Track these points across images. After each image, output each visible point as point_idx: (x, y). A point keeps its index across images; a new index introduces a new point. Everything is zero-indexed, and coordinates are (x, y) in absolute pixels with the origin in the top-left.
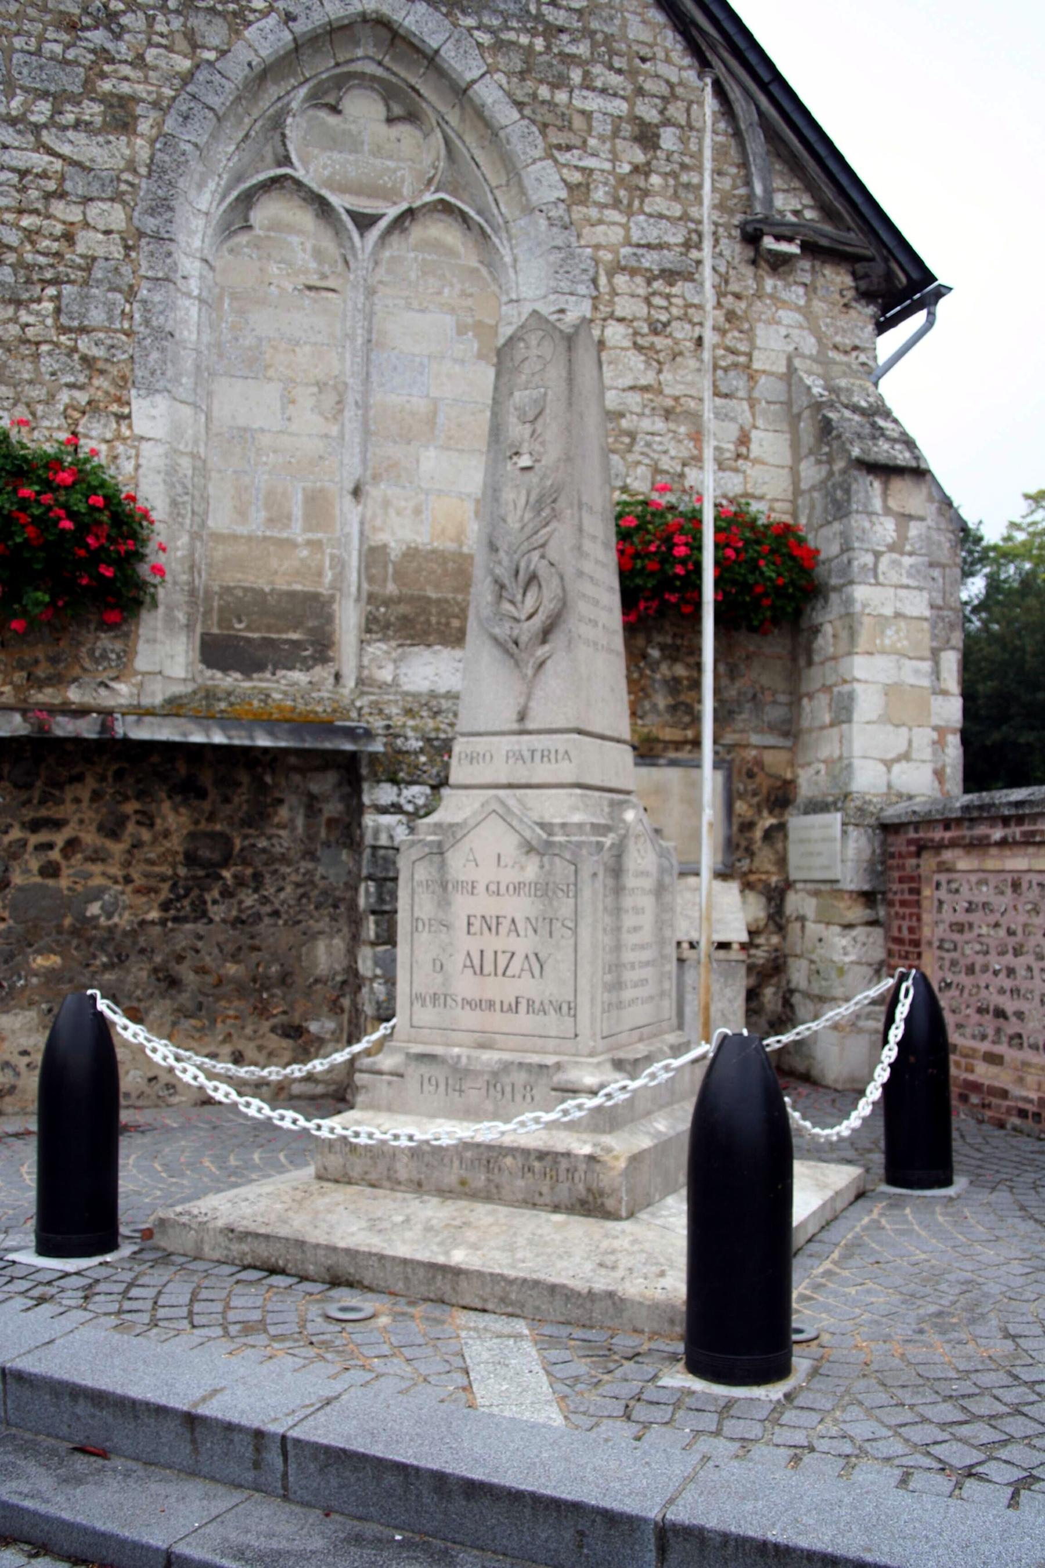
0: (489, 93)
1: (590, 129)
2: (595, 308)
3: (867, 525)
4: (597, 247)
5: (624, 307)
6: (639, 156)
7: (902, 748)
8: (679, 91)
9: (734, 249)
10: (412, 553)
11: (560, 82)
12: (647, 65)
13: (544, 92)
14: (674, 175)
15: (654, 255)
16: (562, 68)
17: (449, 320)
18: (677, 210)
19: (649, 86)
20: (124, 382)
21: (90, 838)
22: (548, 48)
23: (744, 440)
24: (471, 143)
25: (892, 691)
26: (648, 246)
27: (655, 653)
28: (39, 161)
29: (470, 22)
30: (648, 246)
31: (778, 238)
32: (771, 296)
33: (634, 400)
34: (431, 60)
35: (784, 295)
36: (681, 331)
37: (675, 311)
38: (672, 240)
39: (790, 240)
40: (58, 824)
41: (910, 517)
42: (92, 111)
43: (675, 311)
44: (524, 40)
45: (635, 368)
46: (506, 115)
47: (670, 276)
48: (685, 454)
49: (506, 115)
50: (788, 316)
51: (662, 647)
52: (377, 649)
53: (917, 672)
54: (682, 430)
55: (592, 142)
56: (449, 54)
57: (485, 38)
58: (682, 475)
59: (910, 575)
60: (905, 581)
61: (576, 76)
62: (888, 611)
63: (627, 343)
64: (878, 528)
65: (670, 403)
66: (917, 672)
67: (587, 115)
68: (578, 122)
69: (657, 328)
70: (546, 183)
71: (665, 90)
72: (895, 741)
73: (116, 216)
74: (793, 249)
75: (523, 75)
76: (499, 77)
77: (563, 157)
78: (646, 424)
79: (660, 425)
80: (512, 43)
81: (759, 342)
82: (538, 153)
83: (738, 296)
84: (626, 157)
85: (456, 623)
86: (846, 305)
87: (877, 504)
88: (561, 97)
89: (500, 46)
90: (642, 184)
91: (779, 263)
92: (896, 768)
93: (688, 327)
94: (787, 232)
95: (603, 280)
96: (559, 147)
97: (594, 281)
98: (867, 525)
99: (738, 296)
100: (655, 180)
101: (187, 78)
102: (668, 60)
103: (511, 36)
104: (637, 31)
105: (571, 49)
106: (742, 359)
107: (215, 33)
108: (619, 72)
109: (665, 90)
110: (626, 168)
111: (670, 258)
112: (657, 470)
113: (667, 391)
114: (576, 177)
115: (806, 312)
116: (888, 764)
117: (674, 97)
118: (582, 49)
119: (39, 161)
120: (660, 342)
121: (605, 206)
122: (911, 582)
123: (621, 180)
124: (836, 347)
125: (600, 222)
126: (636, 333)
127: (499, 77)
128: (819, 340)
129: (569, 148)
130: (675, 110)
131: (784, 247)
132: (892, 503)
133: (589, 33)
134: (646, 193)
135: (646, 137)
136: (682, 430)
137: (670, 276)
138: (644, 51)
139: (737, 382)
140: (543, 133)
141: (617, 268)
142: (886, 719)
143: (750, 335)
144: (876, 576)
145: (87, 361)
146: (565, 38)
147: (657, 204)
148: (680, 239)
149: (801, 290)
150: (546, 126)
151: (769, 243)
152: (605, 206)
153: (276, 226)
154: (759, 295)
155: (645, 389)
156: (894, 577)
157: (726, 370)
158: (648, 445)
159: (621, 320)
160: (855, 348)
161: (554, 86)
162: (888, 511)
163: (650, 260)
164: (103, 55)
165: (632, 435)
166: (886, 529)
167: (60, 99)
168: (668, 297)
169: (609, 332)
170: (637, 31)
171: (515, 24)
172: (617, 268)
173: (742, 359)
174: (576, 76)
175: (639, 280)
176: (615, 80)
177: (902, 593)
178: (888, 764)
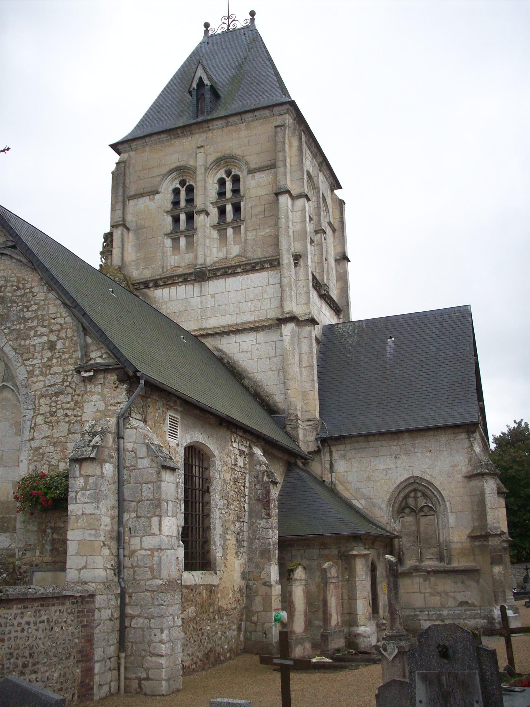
1: (35, 349)
2: (34, 412)
3: (74, 482)
4: (36, 391)
6: (49, 354)
7: (84, 564)
8: (64, 326)
9: (76, 378)
11: (28, 337)
12: (55, 321)
13: (23, 342)
14: (60, 357)
15: (53, 388)
16: (28, 332)
17: (8, 423)
18: (61, 369)
19: (54, 328)
22: (24, 327)
25: (80, 542)
26: (51, 386)
27: (49, 531)
29: (3, 327)
30: (51, 386)
31: (86, 371)
32: (90, 392)
33: (45, 440)
35: (94, 390)
36: (60, 413)
37: (58, 406)
38: (58, 381)
39: (90, 371)
41: (89, 476)
43: (58, 406)
44: (18, 327)
45: (45, 430)
47: (57, 394)
48: (59, 457)
50: (95, 398)
51: (51, 528)
53: (90, 534)
54: (59, 449)
55: (36, 354)
57: (6, 331)
58: (58, 465)
59: (88, 498)
60: (87, 500)
61: (32, 333)
62: (80, 513)
63: (43, 422)
64: (78, 482)
65: (56, 440)
66: (90, 534)
67: (34, 346)
68: (32, 349)
69: (52, 414)
71: (59, 327)
72: (80, 562)
74: (91, 374)
75: (17, 339)
76: (10, 342)
77: (26, 363)
78: (48, 450)
79: (52, 449)
80: (14, 329)
81: (85, 411)
82: (20, 364)
83: (79, 395)
84: (45, 356)
85: (6, 524)
86: (116, 387)
87: (77, 474)
88: (27, 342)
89: (12, 331)
90: (50, 364)
91: (89, 380)
92: (82, 572)
93: (62, 411)
94: (88, 368)
95: (37, 402)
96: (26, 360)
97: (34, 403)
98: (74, 482)
99: (79, 395)
100: (54, 361)
102: (61, 316)
103: (14, 327)
105: (32, 325)
106: (79, 418)
108: (45, 327)
109: (59, 327)
110: (46, 360)
113: (55, 436)
114: (30, 368)
115: (102, 394)
116: (79, 570)
117: (62, 328)
118: (35, 323)
120: (53, 419)
121: (38, 376)
122: (89, 501)
123: (44, 365)
124: (111, 405)
125: (37, 382)
126: (45, 418)
127: (10, 342)
128: (105, 403)
129: (29, 359)
130: (63, 334)
132: (83, 472)
133: (37, 317)
134: (51, 367)
135: (52, 346)
136: (59, 449)
137: (57, 394)
138: (53, 316)
139: (77, 427)
140: (22, 357)
141: (43, 396)
142: (77, 554)
143: (82, 408)
144: (76, 501)
146: (30, 321)
147: (55, 369)
148: (61, 380)
149: (100, 386)
150: (23, 354)
151: (83, 374)
152: (38, 376)
154: (86, 392)
155: (48, 437)
156: (83, 500)
157: (73, 423)
158: (48, 457)
159: (41, 415)
160: (119, 403)
161: (25, 340)
162: (81, 475)
163: (52, 390)
165: (43, 454)
166: (81, 482)
168: (56, 402)
169: (37, 420)
170: (52, 310)
171: (15, 323)
173: (79, 418)
174: (32, 333)
175: (48, 398)
176: (44, 330)
177: (85, 505)
178: (79, 570)
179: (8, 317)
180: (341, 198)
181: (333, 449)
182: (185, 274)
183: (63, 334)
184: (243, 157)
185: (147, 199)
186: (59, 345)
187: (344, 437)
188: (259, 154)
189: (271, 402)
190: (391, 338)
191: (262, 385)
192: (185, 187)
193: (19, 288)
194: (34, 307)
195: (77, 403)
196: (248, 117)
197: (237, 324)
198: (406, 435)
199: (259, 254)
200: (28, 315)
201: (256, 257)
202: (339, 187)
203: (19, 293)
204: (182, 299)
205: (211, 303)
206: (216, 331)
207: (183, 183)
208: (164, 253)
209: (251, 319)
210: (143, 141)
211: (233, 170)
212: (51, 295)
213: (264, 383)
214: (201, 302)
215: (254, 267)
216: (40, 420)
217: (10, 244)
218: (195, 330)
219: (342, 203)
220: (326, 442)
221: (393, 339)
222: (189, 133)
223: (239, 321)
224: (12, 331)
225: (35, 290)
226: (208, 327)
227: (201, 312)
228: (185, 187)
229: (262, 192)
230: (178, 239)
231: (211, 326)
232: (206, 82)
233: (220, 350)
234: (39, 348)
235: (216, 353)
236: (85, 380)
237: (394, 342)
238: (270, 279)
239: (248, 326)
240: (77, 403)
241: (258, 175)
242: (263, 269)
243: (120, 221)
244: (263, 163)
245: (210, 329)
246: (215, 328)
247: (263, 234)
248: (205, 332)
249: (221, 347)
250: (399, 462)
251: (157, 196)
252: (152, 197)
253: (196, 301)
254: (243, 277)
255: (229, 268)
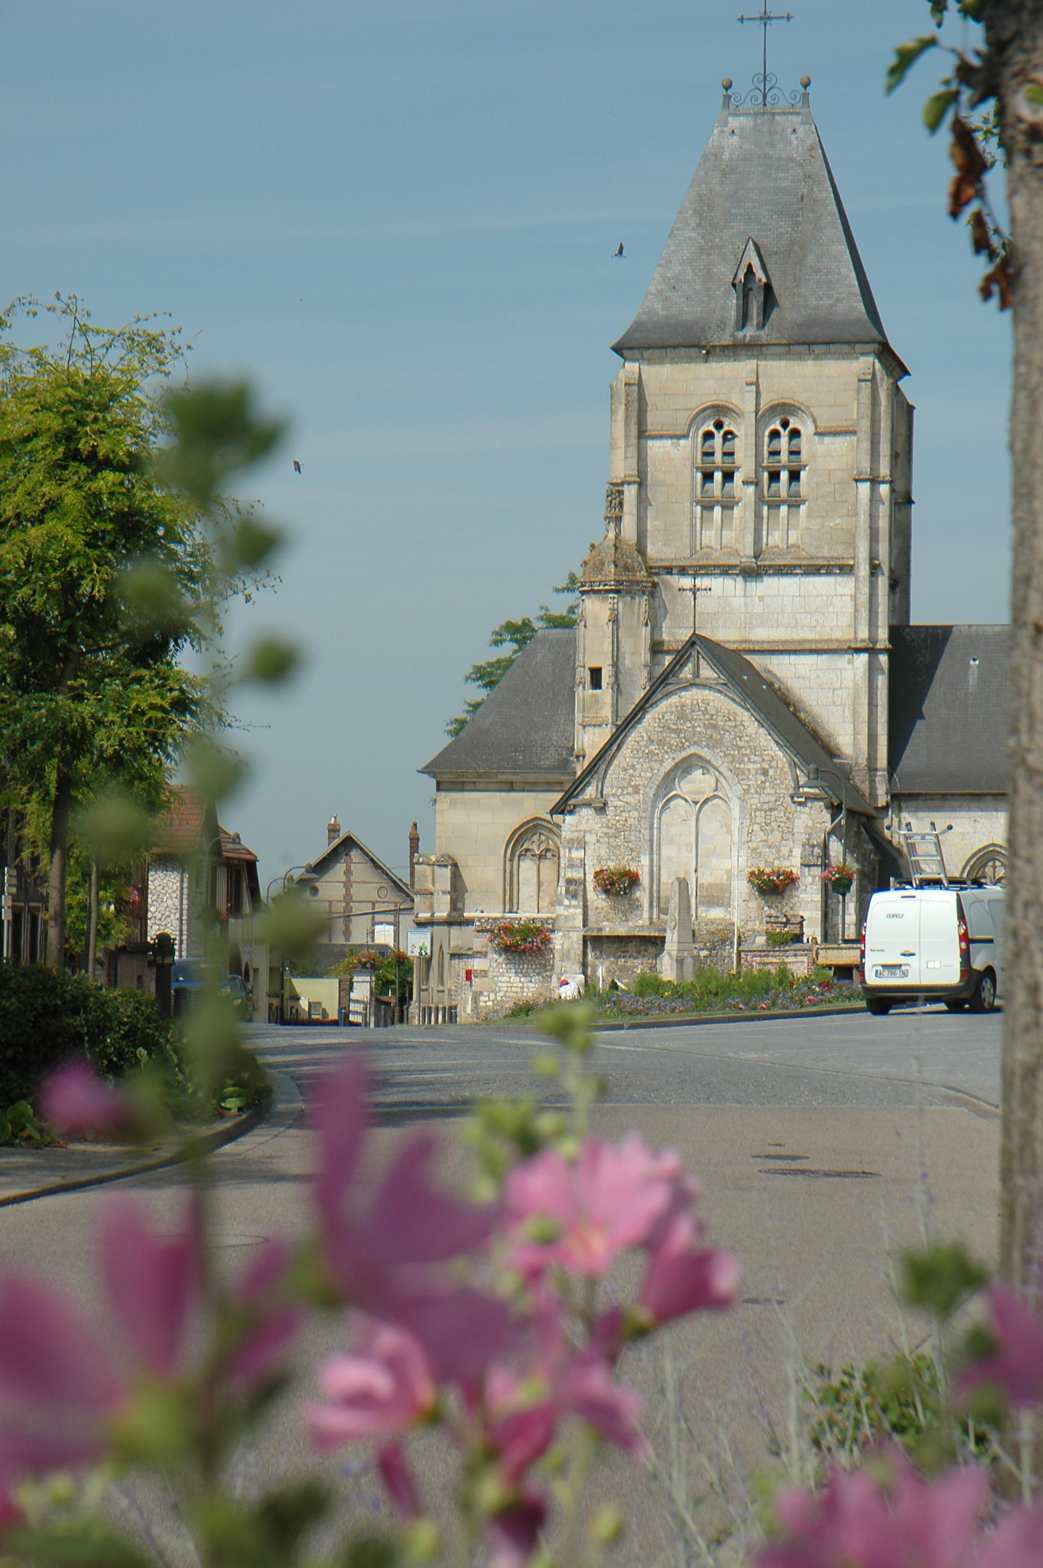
0: (723, 769)
5: (758, 820)
6: (763, 778)
10: (710, 885)
17: (719, 825)
19: (766, 758)
20: (639, 853)
21: (635, 955)
23: (791, 851)
24: (721, 778)
28: (619, 803)
33: (761, 844)
34: (709, 762)
36: (774, 825)
40: (627, 952)
42: (630, 790)
46: (727, 774)
47: (771, 810)
49: (727, 774)
50: (803, 816)
52: (701, 909)
56: (712, 761)
61: (746, 760)
67: (749, 770)
68: (746, 772)
70: (739, 790)
73: (636, 814)
88: (742, 766)
91: (800, 804)
101: (651, 778)
104: (763, 743)
107: (656, 766)
111: (771, 805)
112: (766, 861)
115: (810, 814)
119: (619, 803)
130: (774, 764)
131: (800, 800)
135: (765, 773)
137: (771, 810)
141: (757, 809)
145: (631, 849)
153: (675, 805)
163: (766, 806)
164: (632, 776)
167: (623, 788)
172: (757, 809)
176: (757, 758)
179: (722, 743)
180: (911, 403)
181: (903, 805)
182: (724, 566)
183: (774, 764)
184: (808, 408)
185: (668, 443)
186: (771, 772)
187: (918, 795)
188: (830, 407)
189: (832, 744)
190: (974, 660)
191: (822, 722)
192: (722, 432)
193: (730, 720)
194: (747, 739)
195: (788, 818)
196: (819, 349)
197: (793, 642)
198: (989, 797)
199: (825, 552)
200: (740, 744)
201: (820, 555)
202: (906, 372)
203: (730, 723)
204: (719, 597)
205: (759, 608)
206: (766, 647)
207: (719, 425)
208: (693, 526)
209: (811, 636)
210: (663, 351)
211: (791, 421)
212: (762, 731)
213: (825, 719)
214: (746, 604)
215: (819, 569)
216: (756, 827)
217: (721, 681)
218: (735, 642)
219: (911, 409)
220: (899, 799)
221: (977, 662)
222: (731, 353)
223: (796, 637)
224: (726, 755)
225: (746, 724)
226: (753, 639)
227: (745, 618)
228: (722, 432)
229: (833, 465)
230: (712, 508)
231: (758, 639)
232: (759, 274)
233: (769, 672)
234: (753, 772)
235: (764, 675)
236: (800, 804)
237: (978, 666)
238: (838, 588)
239: (807, 646)
240: (788, 818)
241: (827, 439)
242: (829, 573)
243: (632, 476)
244: (835, 424)
245: (758, 642)
246: (763, 642)
247: (832, 524)
248: (751, 647)
249: (770, 667)
250: (978, 826)
251: (682, 442)
252: (674, 441)
253: (738, 602)
254: (803, 579)
255: (785, 566)
